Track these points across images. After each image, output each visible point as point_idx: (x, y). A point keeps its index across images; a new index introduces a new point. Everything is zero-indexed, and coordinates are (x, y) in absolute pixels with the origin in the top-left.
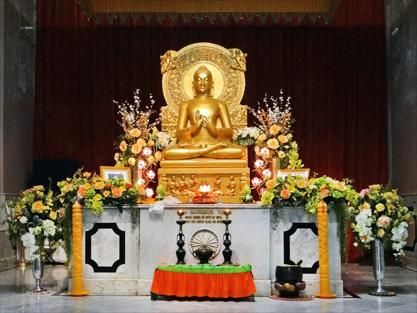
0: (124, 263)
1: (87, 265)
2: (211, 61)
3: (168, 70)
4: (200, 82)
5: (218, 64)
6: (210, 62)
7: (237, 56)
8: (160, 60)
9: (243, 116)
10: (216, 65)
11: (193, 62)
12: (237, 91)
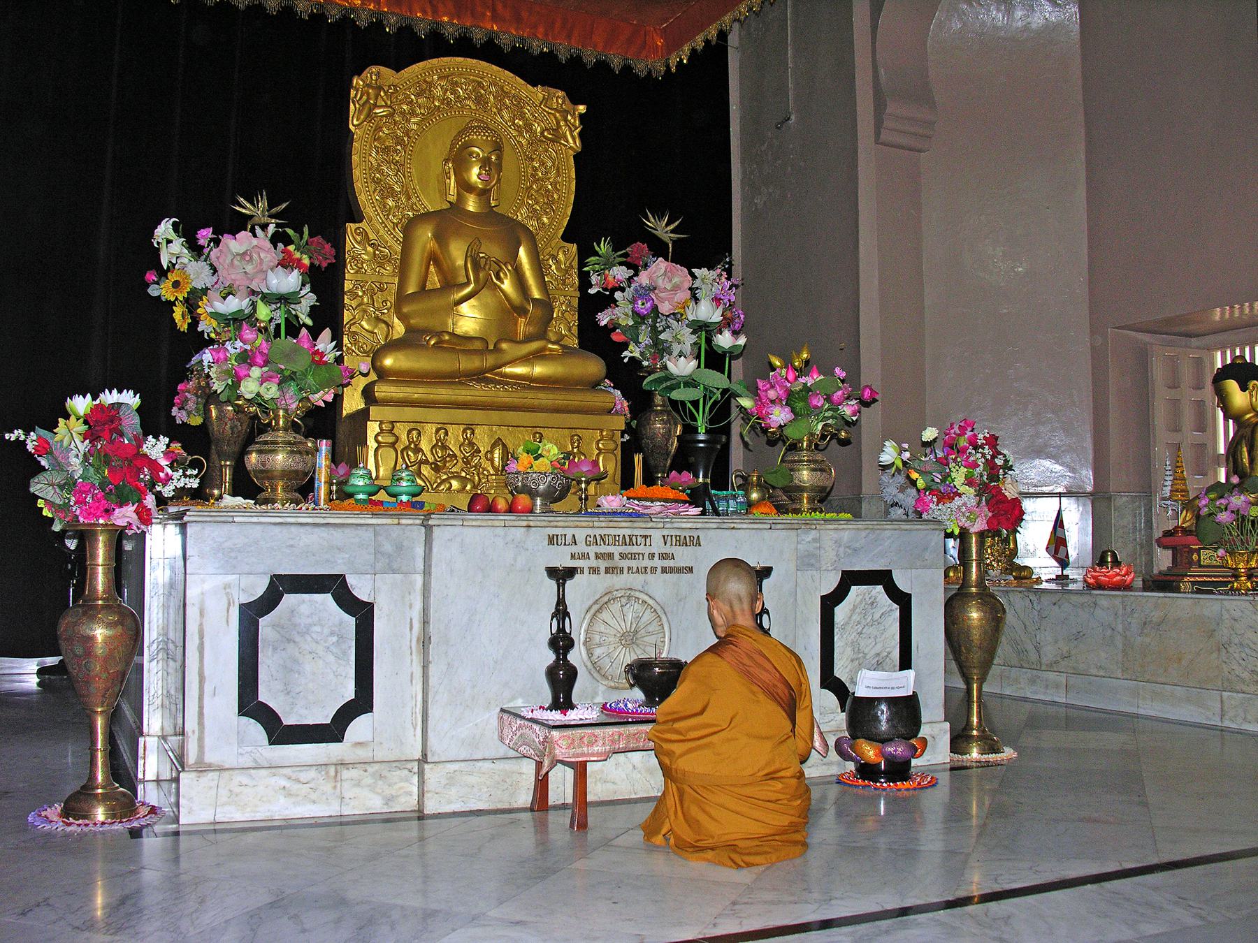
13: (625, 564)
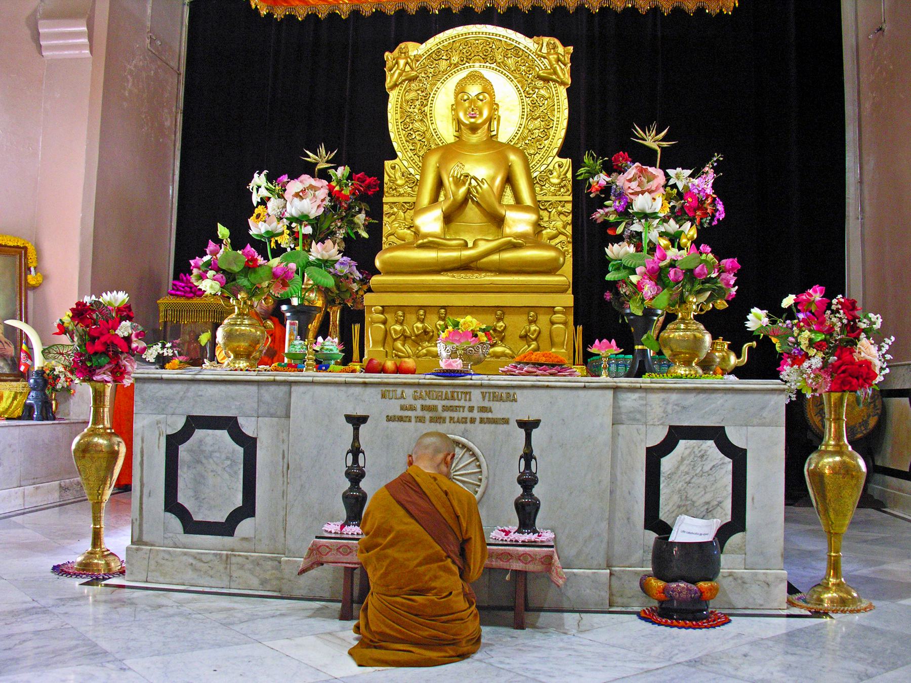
0: (252, 514)
1: (169, 514)
2: (495, 64)
3: (401, 83)
6: (492, 65)
7: (550, 51)
8: (384, 63)
9: (562, 181)
10: (505, 72)
11: (455, 65)
12: (551, 126)
13: (447, 415)
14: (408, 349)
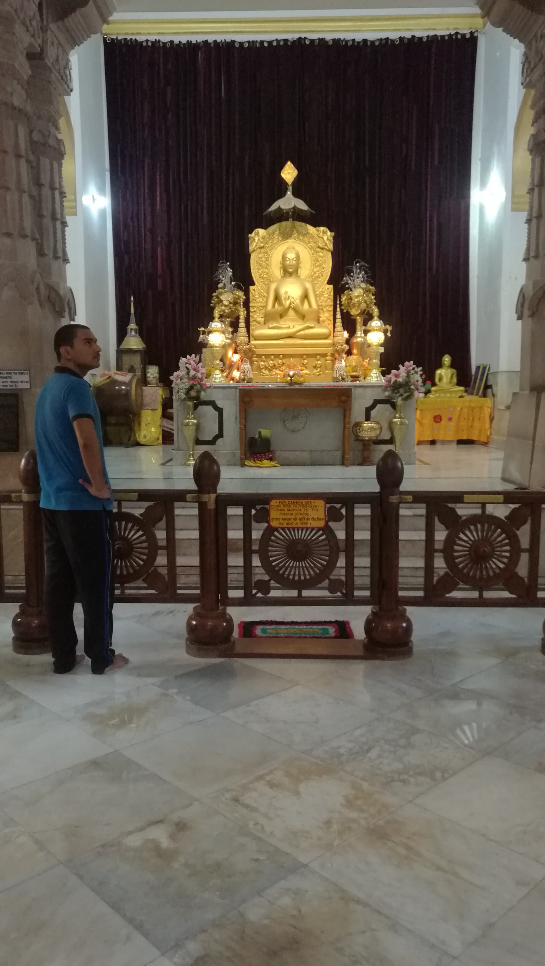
3: (257, 249)
4: (288, 262)
5: (305, 242)
8: (248, 239)
14: (267, 372)
